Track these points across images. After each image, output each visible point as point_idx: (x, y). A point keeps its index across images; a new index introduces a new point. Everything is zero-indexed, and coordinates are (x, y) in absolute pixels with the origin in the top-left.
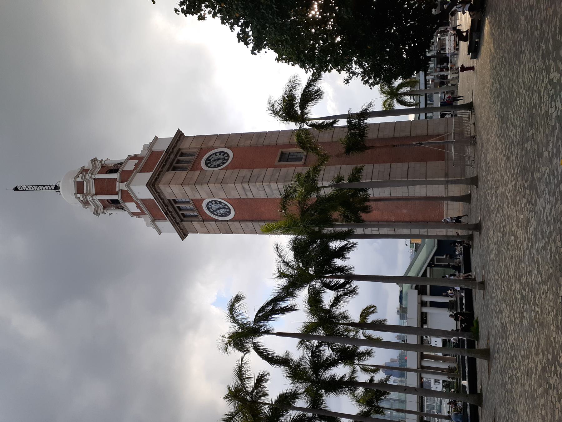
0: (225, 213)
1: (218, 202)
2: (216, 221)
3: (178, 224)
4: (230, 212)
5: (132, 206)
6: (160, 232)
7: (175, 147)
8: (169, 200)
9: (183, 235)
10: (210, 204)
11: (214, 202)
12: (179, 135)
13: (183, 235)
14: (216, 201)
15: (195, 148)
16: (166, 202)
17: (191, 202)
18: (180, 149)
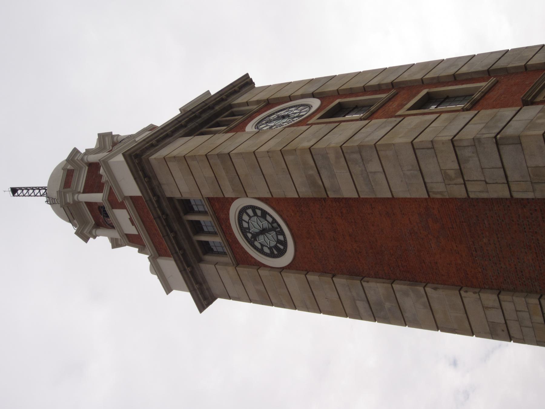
0: (276, 247)
1: (259, 212)
2: (260, 265)
3: (188, 266)
4: (284, 243)
5: (122, 216)
6: (168, 290)
7: (222, 100)
8: (171, 200)
9: (203, 300)
10: (245, 217)
11: (250, 212)
12: (245, 83)
13: (203, 300)
14: (254, 208)
15: (258, 102)
16: (165, 204)
17: (208, 208)
18: (231, 106)
